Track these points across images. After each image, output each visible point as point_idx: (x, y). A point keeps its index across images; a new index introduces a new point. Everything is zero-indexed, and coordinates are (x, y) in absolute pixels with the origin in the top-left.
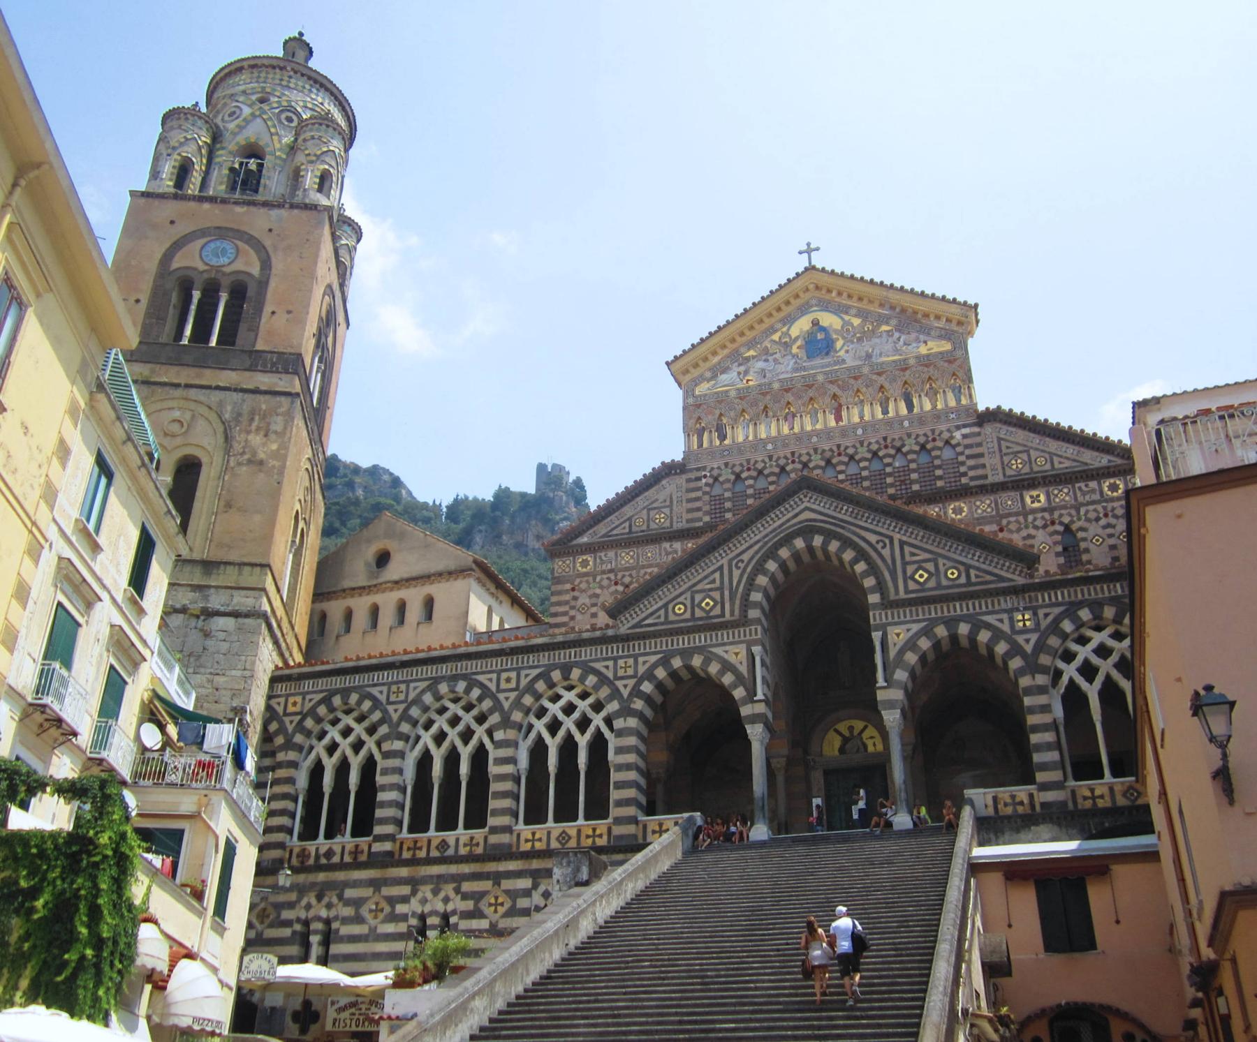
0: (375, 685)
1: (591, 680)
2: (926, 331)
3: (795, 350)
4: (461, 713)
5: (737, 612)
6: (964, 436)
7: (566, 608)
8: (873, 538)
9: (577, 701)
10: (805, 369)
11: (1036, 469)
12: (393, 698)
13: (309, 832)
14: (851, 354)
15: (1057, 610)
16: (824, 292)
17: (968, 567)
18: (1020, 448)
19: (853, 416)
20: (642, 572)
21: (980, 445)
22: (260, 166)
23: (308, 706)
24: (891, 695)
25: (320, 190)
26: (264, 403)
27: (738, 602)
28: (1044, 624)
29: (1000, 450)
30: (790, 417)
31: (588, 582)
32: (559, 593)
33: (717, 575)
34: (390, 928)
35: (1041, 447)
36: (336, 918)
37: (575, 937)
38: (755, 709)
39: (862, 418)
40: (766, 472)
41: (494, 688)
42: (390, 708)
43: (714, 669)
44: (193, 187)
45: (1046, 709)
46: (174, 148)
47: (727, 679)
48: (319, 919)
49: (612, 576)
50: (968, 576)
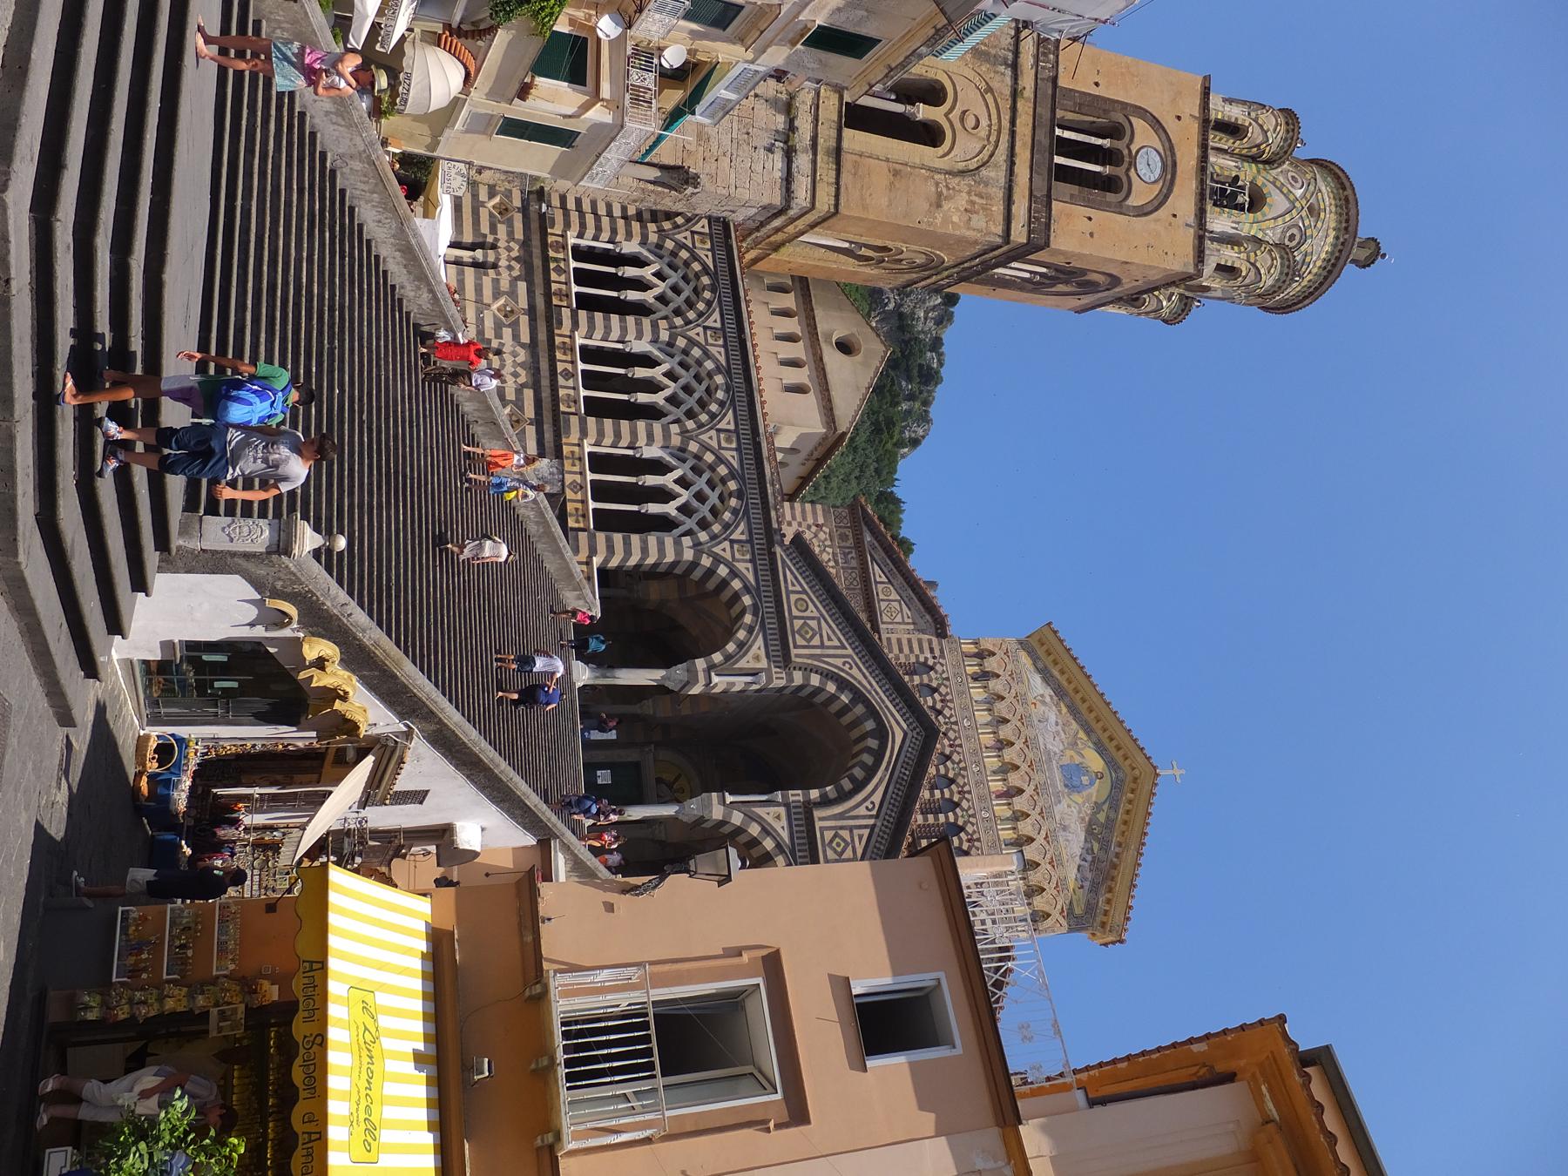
0: (722, 315)
1: (727, 516)
2: (1094, 888)
3: (1070, 753)
4: (696, 396)
7: (799, 518)
13: (580, 254)
16: (1132, 785)
22: (1240, 208)
23: (701, 254)
25: (1220, 268)
26: (998, 209)
32: (814, 513)
33: (837, 643)
34: (489, 324)
36: (499, 274)
37: (485, 434)
43: (741, 634)
44: (1217, 140)
46: (1256, 120)
47: (731, 647)
48: (498, 259)
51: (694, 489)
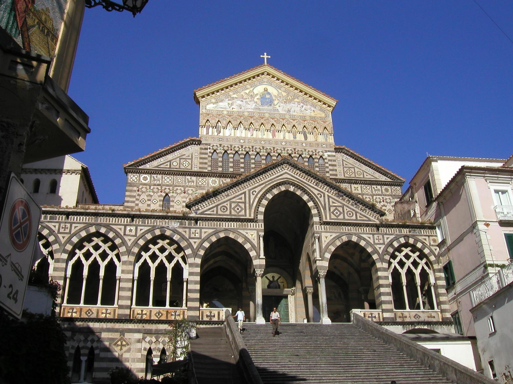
3: (255, 100)
4: (101, 244)
5: (252, 215)
6: (329, 156)
7: (134, 199)
8: (316, 192)
9: (167, 246)
10: (259, 109)
11: (357, 176)
12: (62, 230)
14: (281, 108)
15: (392, 237)
17: (356, 212)
18: (351, 166)
19: (280, 136)
20: (175, 188)
21: (335, 161)
27: (253, 211)
28: (387, 241)
31: (146, 188)
32: (131, 191)
33: (243, 196)
38: (259, 262)
39: (284, 138)
40: (239, 153)
41: (123, 234)
42: (60, 236)
43: (240, 240)
45: (387, 278)
47: (247, 246)
49: (159, 188)
50: (356, 216)
51: (158, 252)
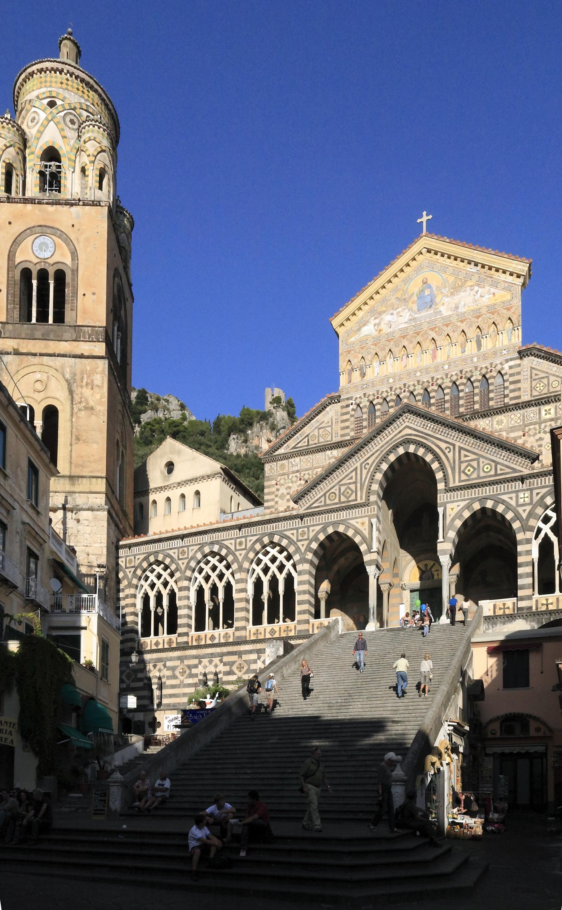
6: (511, 367)
18: (544, 375)
19: (441, 356)
21: (519, 373)
24: (445, 547)
29: (531, 378)
30: (405, 357)
35: (557, 374)
